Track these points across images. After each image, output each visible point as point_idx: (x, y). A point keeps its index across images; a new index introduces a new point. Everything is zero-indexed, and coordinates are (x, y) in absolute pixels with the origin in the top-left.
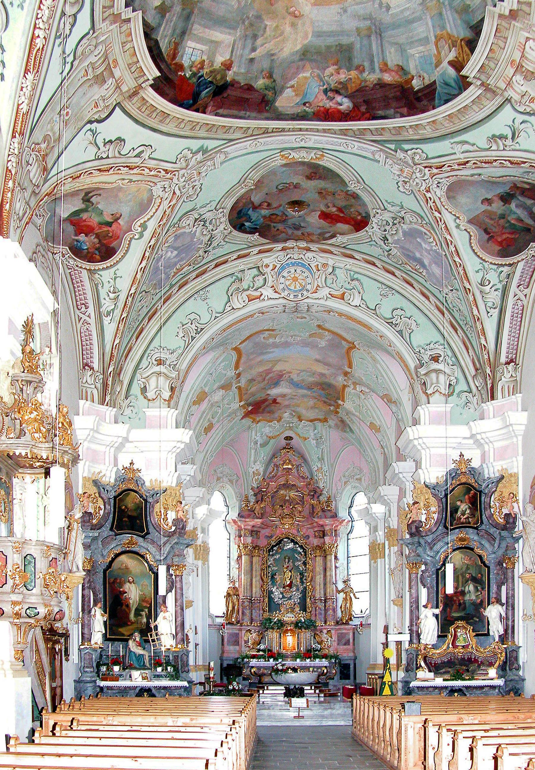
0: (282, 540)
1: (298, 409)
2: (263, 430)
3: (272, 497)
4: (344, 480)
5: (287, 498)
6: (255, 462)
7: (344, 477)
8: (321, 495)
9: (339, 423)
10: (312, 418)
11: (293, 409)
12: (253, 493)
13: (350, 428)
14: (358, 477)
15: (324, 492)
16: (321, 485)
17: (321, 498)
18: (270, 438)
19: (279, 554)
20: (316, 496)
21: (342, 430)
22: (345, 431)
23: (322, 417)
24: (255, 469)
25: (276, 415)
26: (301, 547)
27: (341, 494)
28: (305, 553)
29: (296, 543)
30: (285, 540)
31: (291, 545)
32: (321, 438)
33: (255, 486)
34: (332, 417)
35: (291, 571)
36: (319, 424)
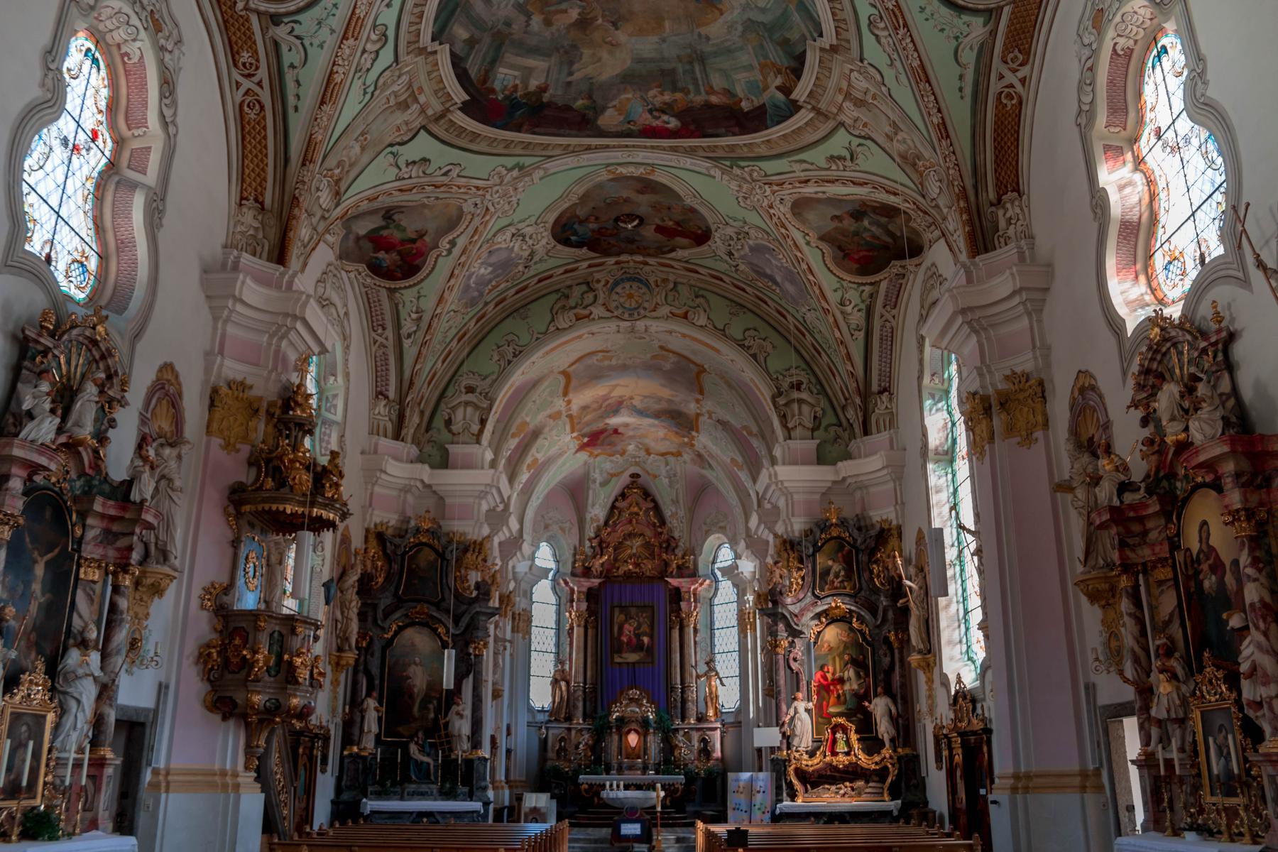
4: (705, 528)
6: (593, 505)
8: (677, 546)
16: (676, 535)
18: (612, 475)
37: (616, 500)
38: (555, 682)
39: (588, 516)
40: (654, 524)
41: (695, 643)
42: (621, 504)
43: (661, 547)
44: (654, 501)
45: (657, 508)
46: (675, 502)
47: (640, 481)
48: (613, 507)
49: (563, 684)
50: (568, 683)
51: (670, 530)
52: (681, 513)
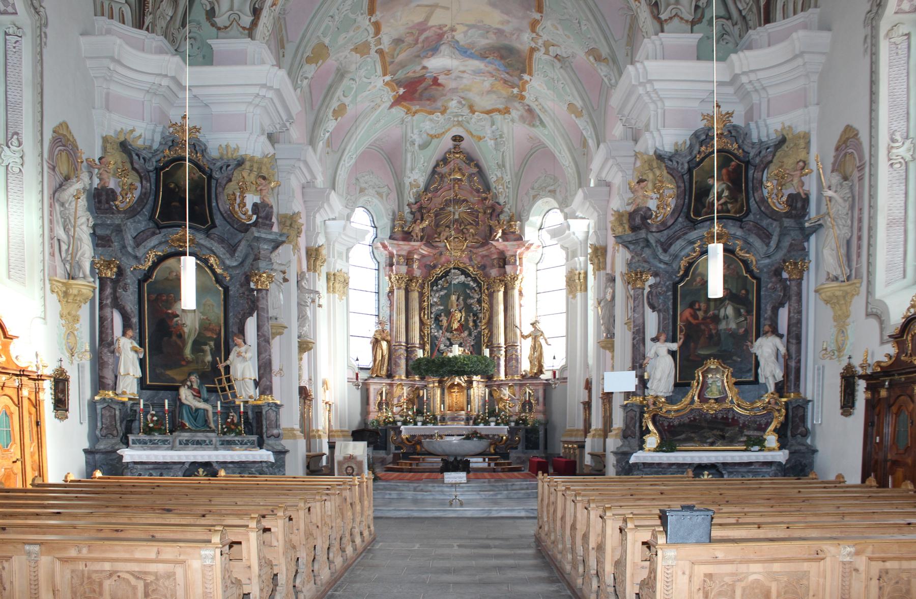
0: (449, 271)
1: (470, 95)
2: (421, 125)
3: (436, 216)
4: (532, 193)
5: (457, 217)
6: (412, 170)
7: (533, 189)
8: (502, 212)
9: (525, 114)
10: (489, 108)
11: (462, 95)
12: (409, 210)
13: (541, 120)
14: (552, 188)
15: (506, 209)
16: (502, 200)
17: (502, 217)
18: (433, 137)
19: (445, 289)
20: (495, 214)
21: (529, 124)
22: (534, 126)
23: (501, 107)
24: (411, 180)
25: (439, 104)
26: (475, 280)
27: (529, 212)
28: (480, 288)
29: (467, 275)
30: (453, 271)
31: (462, 278)
32: (501, 136)
33: (412, 200)
34: (516, 104)
35: (460, 311)
36: (498, 117)
37: (437, 165)
38: (376, 342)
39: (407, 181)
40: (478, 191)
41: (521, 306)
42: (443, 170)
43: (485, 213)
44: (477, 166)
45: (481, 172)
46: (501, 166)
47: (463, 145)
48: (434, 172)
49: (384, 344)
50: (388, 342)
51: (496, 196)
52: (507, 178)
